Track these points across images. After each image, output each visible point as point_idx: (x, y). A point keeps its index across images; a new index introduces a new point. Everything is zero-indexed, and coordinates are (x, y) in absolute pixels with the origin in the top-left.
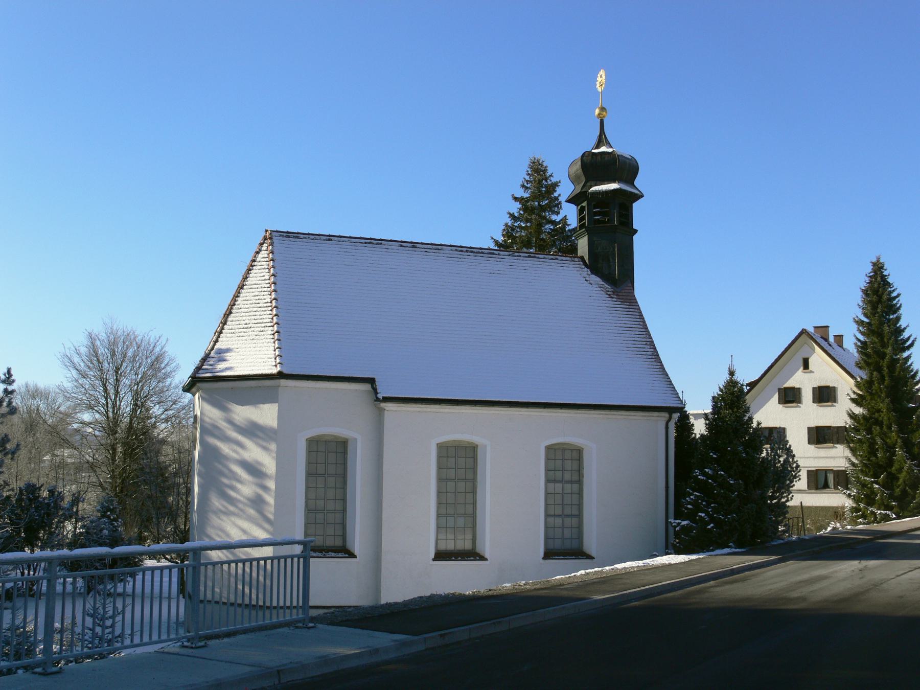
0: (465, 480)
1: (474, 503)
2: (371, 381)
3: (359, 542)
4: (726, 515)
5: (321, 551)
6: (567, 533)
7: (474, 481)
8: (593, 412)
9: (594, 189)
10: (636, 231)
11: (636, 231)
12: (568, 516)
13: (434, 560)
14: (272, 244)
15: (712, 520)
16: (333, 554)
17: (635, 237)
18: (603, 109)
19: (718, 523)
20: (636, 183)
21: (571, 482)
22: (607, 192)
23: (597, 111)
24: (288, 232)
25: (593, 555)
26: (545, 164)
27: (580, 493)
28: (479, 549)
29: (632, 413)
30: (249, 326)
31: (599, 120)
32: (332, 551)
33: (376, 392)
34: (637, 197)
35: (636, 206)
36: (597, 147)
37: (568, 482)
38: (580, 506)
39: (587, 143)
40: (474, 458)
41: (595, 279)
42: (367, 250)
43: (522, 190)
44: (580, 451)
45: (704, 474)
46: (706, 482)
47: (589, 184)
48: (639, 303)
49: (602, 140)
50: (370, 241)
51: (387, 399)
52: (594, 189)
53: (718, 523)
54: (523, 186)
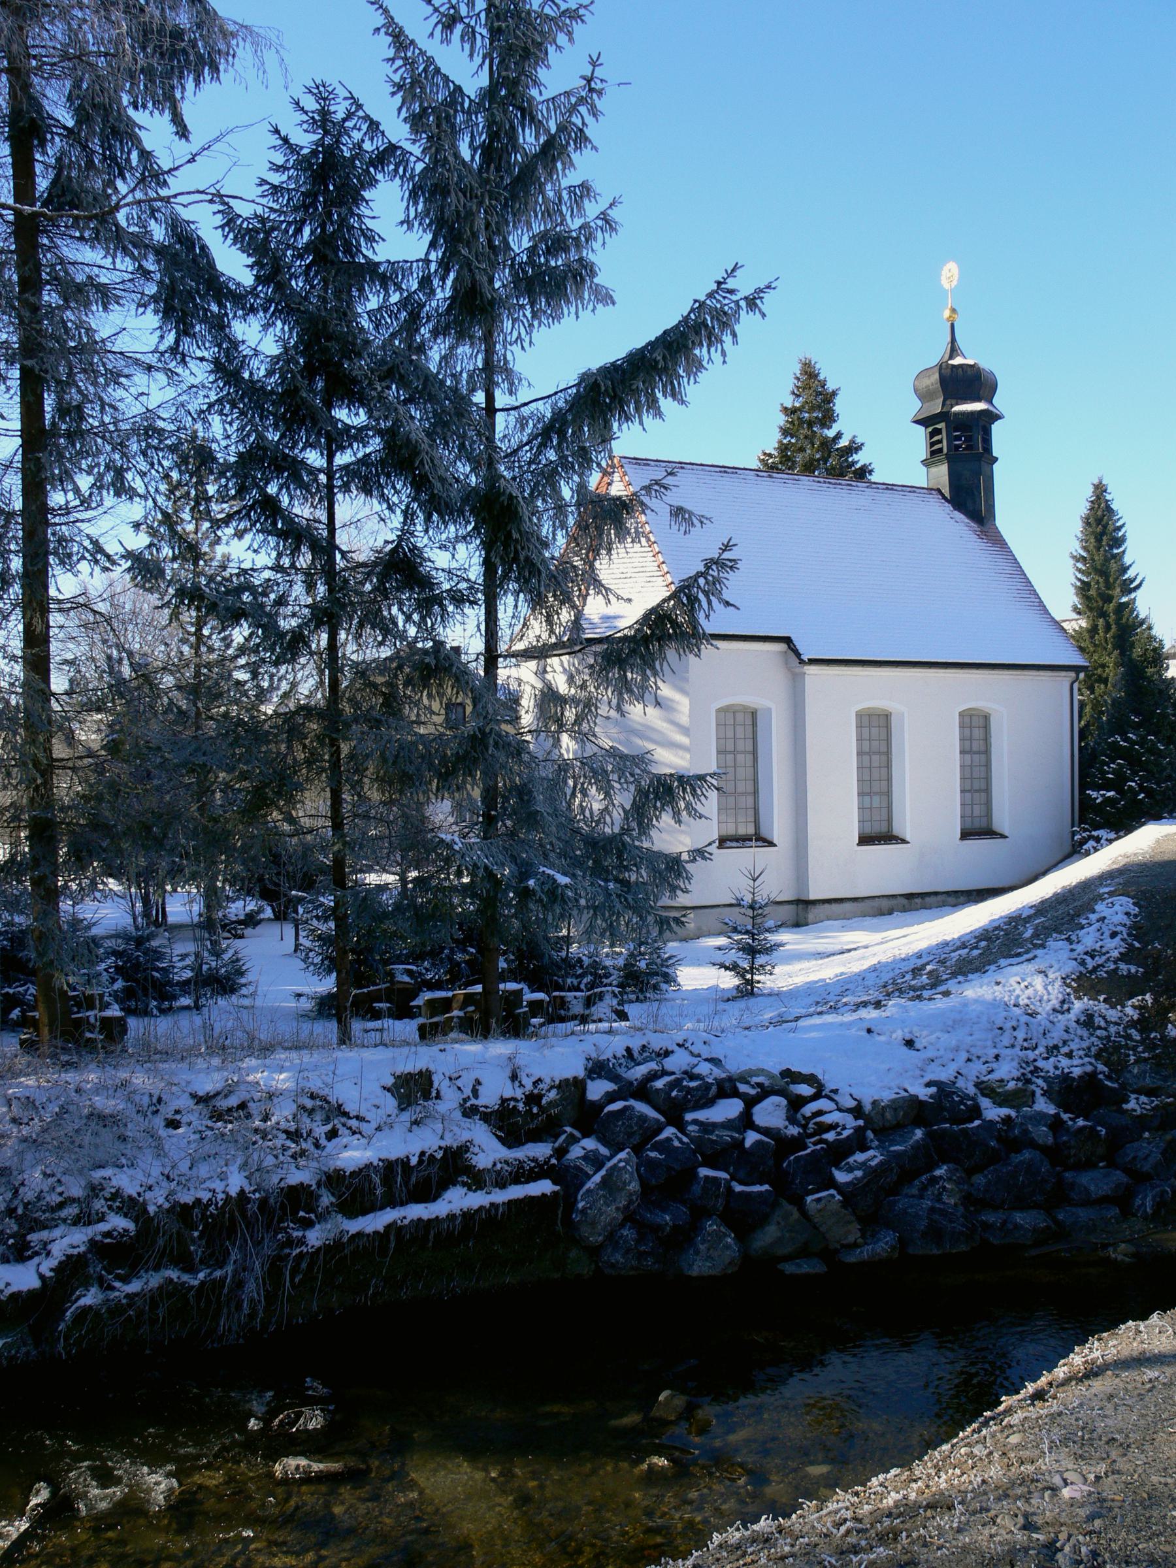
0: (879, 753)
1: (889, 780)
2: (787, 640)
3: (779, 827)
4: (1158, 784)
5: (737, 840)
6: (977, 812)
7: (888, 753)
8: (1006, 672)
9: (957, 408)
10: (996, 459)
11: (996, 459)
12: (976, 791)
13: (859, 844)
14: (625, 474)
15: (1142, 789)
16: (734, 844)
17: (995, 466)
18: (953, 310)
19: (1149, 793)
20: (994, 401)
21: (979, 753)
22: (972, 413)
23: (947, 313)
24: (635, 459)
25: (1006, 834)
26: (817, 367)
27: (988, 765)
28: (896, 831)
29: (1041, 673)
30: (628, 575)
31: (949, 324)
32: (731, 840)
33: (797, 654)
34: (998, 417)
35: (996, 428)
36: (951, 358)
37: (975, 753)
38: (988, 779)
39: (934, 354)
40: (888, 727)
41: (958, 515)
42: (724, 480)
43: (792, 397)
44: (986, 718)
45: (1126, 740)
46: (1132, 748)
47: (948, 402)
48: (1010, 545)
49: (954, 350)
50: (725, 469)
51: (812, 661)
52: (957, 408)
53: (1149, 793)
54: (793, 393)
